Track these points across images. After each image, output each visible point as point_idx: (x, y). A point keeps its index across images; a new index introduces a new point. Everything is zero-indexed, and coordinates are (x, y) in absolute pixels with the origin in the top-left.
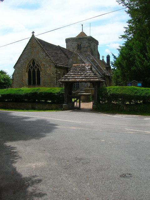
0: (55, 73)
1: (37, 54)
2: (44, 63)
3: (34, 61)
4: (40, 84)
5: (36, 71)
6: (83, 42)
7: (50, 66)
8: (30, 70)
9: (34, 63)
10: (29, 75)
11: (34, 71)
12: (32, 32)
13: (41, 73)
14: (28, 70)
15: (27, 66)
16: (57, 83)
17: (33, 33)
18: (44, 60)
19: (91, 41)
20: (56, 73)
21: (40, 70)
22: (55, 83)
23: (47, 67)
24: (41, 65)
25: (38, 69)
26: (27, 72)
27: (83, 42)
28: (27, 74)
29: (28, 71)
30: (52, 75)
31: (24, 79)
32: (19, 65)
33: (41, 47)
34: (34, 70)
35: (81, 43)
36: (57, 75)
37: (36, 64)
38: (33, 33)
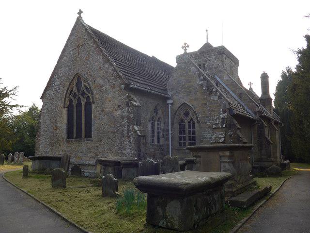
2: (101, 81)
3: (79, 78)
5: (83, 102)
7: (113, 87)
8: (71, 101)
9: (79, 84)
11: (79, 105)
12: (82, 10)
13: (93, 106)
14: (67, 103)
16: (129, 131)
17: (80, 12)
18: (101, 73)
19: (225, 56)
20: (127, 105)
21: (91, 101)
22: (125, 132)
23: (106, 91)
24: (93, 87)
26: (64, 107)
28: (65, 112)
31: (59, 124)
32: (51, 92)
33: (95, 42)
34: (79, 99)
35: (206, 61)
36: (128, 111)
38: (80, 12)
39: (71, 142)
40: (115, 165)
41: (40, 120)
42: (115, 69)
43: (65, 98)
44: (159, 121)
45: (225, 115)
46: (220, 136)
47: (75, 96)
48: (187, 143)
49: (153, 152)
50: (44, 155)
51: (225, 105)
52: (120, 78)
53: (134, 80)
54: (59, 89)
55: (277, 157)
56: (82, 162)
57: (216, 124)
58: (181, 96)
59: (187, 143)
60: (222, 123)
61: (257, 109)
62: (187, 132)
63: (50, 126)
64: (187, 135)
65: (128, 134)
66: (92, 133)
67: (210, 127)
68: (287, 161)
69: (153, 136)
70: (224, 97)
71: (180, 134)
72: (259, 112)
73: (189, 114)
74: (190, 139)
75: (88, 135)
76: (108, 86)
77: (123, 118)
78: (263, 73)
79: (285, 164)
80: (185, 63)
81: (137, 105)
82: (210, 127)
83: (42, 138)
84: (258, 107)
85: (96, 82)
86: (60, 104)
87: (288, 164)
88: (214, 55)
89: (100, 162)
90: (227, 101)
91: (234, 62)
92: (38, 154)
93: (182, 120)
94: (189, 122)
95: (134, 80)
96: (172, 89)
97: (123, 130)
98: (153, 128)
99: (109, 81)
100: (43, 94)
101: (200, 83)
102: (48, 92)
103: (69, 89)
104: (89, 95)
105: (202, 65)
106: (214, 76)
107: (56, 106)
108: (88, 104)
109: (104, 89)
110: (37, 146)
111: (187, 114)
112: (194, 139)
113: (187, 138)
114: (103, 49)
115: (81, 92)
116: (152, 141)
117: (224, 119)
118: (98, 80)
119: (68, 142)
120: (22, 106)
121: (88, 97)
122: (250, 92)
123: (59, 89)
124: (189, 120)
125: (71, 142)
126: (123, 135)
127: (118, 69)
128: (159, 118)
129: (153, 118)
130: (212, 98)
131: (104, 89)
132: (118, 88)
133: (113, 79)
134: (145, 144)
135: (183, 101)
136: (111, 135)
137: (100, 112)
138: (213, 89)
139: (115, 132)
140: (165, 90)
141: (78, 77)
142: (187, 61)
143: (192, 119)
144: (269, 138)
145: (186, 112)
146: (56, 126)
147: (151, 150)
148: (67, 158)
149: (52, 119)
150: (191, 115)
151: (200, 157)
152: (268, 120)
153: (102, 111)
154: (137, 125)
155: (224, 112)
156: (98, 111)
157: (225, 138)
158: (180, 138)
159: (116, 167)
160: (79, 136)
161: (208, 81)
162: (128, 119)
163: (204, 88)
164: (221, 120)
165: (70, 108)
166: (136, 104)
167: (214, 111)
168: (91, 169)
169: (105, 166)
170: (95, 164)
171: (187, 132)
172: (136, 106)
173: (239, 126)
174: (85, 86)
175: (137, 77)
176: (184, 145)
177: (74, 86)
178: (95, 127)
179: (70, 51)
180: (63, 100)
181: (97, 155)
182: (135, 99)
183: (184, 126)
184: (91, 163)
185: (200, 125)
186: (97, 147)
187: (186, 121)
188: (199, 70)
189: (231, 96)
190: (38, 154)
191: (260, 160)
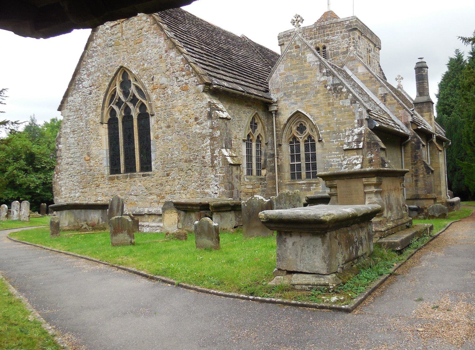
0: (204, 116)
1: (137, 46)
2: (164, 80)
4: (149, 169)
5: (135, 113)
6: (331, 37)
7: (185, 89)
8: (112, 112)
9: (125, 85)
10: (109, 128)
11: (128, 118)
13: (152, 120)
15: (101, 101)
16: (213, 158)
18: (163, 65)
19: (357, 34)
20: (210, 116)
21: (149, 111)
22: (208, 159)
25: (143, 106)
26: (102, 123)
27: (331, 37)
28: (104, 131)
29: (106, 120)
30: (196, 129)
31: (94, 151)
34: (127, 110)
35: (327, 42)
36: (212, 128)
37: (133, 89)
39: (116, 180)
40: (201, 210)
41: (60, 146)
42: (186, 59)
43: (103, 109)
44: (258, 141)
45: (362, 129)
46: (355, 161)
47: (119, 103)
48: (304, 173)
49: (251, 191)
50: (70, 201)
51: (361, 113)
52: (197, 74)
53: (218, 76)
54: (90, 94)
55: (440, 193)
56: (137, 210)
57: (349, 144)
58: (293, 101)
59: (304, 173)
60: (358, 141)
61: (410, 119)
62: (303, 156)
63: (78, 154)
64: (303, 163)
65: (212, 162)
66: (153, 163)
67: (338, 149)
68: (457, 199)
69: (249, 165)
70: (359, 101)
71: (293, 160)
72: (413, 122)
73: (305, 128)
74: (308, 168)
75: (146, 166)
76: (177, 89)
77: (203, 137)
78: (420, 61)
79: (452, 204)
80: (297, 47)
81: (225, 116)
82: (338, 149)
83: (64, 175)
84: (412, 115)
85: (155, 80)
86: (94, 117)
87: (458, 202)
88: (341, 32)
89: (168, 205)
90: (365, 107)
91: (373, 43)
92: (59, 200)
93: (295, 138)
94: (306, 141)
95: (218, 76)
96: (278, 90)
97: (203, 157)
98: (249, 151)
99: (177, 78)
100: (62, 102)
101: (323, 79)
102: (70, 99)
103: (109, 93)
104: (144, 101)
105: (321, 49)
106: (342, 67)
107: (87, 122)
108: (144, 117)
109: (170, 92)
110: (56, 187)
111: (301, 129)
112: (315, 167)
113: (303, 165)
114: (165, 26)
115: (130, 97)
116: (250, 172)
117: (360, 134)
118: (157, 77)
119: (111, 179)
120: (16, 123)
121: (143, 105)
122: (398, 93)
123: (90, 94)
124: (306, 139)
125: (116, 180)
126: (204, 165)
127: (190, 59)
128: (258, 137)
129: (249, 136)
130: (341, 104)
131: (170, 92)
132: (193, 91)
133: (184, 76)
134: (239, 177)
135: (296, 108)
136: (184, 165)
137: (164, 129)
138: (341, 89)
139: (190, 161)
140: (267, 91)
141: (124, 72)
142: (300, 45)
143: (310, 137)
144: (429, 164)
145: (301, 124)
146: (89, 154)
147: (247, 187)
148: (119, 203)
149: (81, 143)
150: (308, 130)
151: (336, 187)
152: (426, 135)
153: (169, 127)
154: (226, 148)
155: (361, 123)
156: (161, 128)
157: (362, 163)
158: (292, 166)
159: (202, 212)
160: (130, 168)
161: (334, 76)
162: (211, 139)
163: (328, 88)
164: (356, 137)
165: (112, 123)
166: (225, 115)
167: (344, 123)
168: (154, 221)
169: (186, 211)
170: (161, 212)
171: (303, 156)
172: (223, 118)
173: (383, 146)
174: (137, 88)
175: (222, 72)
176: (300, 177)
177: (118, 87)
178: (158, 153)
179: (107, 29)
180: (99, 110)
181: (163, 198)
182: (220, 106)
183: (298, 150)
184: (153, 210)
185: (323, 146)
186: (161, 185)
187: (301, 140)
188: (320, 59)
189: (370, 100)
190: (59, 200)
191: (416, 198)
